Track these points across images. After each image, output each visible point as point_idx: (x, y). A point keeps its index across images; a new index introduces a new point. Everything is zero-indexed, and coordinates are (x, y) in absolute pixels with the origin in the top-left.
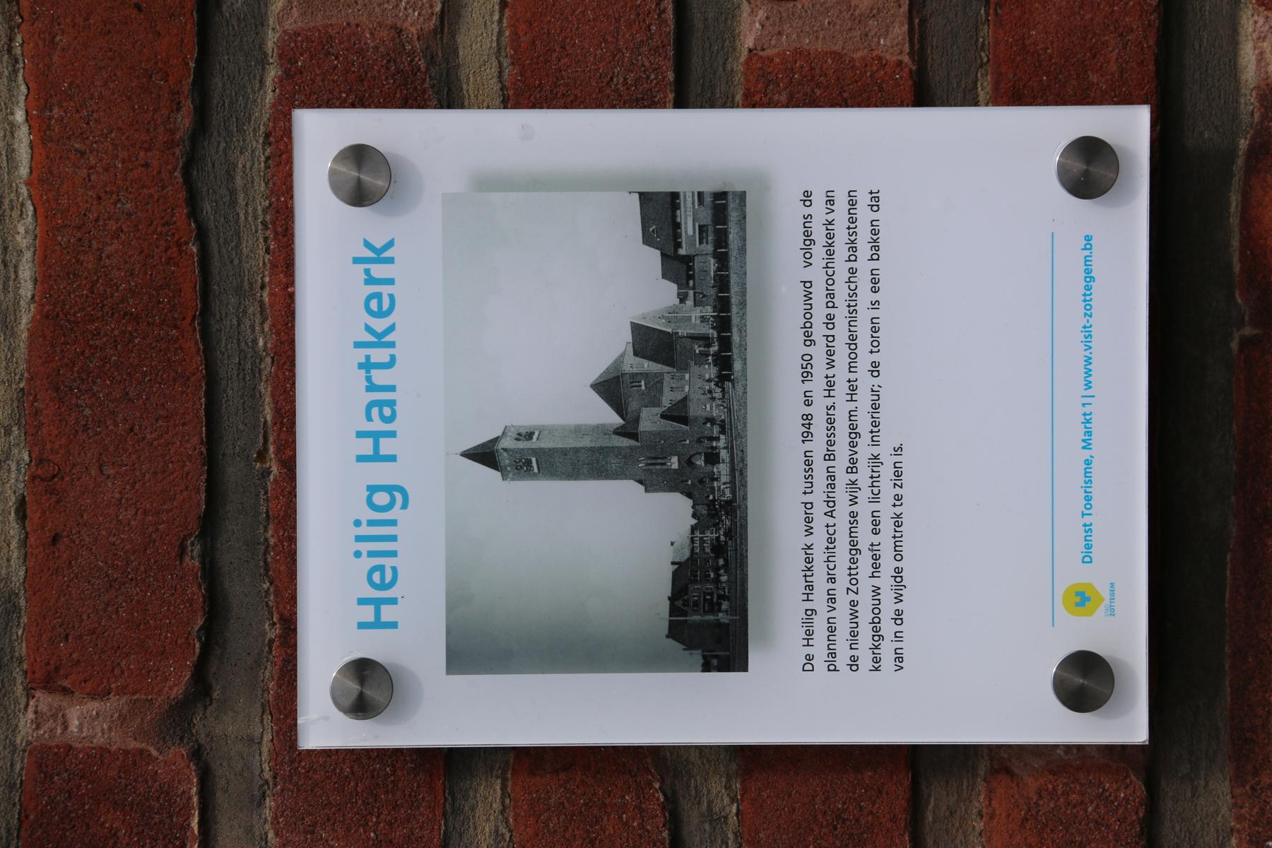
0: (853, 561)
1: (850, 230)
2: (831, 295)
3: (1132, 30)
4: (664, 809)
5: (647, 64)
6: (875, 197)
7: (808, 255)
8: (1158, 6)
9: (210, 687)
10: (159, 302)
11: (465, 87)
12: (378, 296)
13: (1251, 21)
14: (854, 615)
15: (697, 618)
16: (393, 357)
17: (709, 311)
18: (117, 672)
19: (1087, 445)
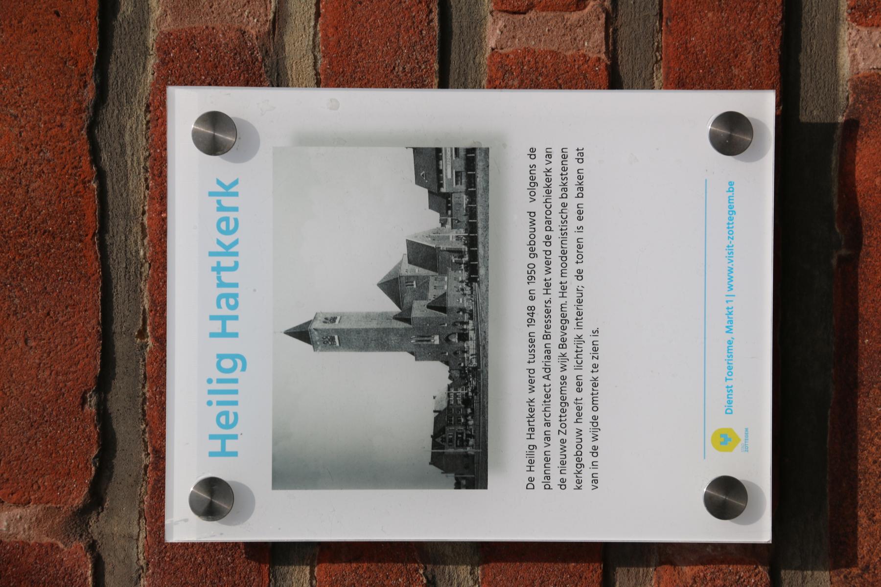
0: (563, 411)
1: (563, 176)
2: (549, 222)
3: (763, 38)
5: (419, 58)
6: (580, 153)
8: (781, 22)
10: (69, 223)
11: (289, 72)
12: (227, 219)
13: (847, 33)
14: (563, 449)
15: (451, 450)
16: (236, 263)
17: (462, 232)
19: (729, 330)
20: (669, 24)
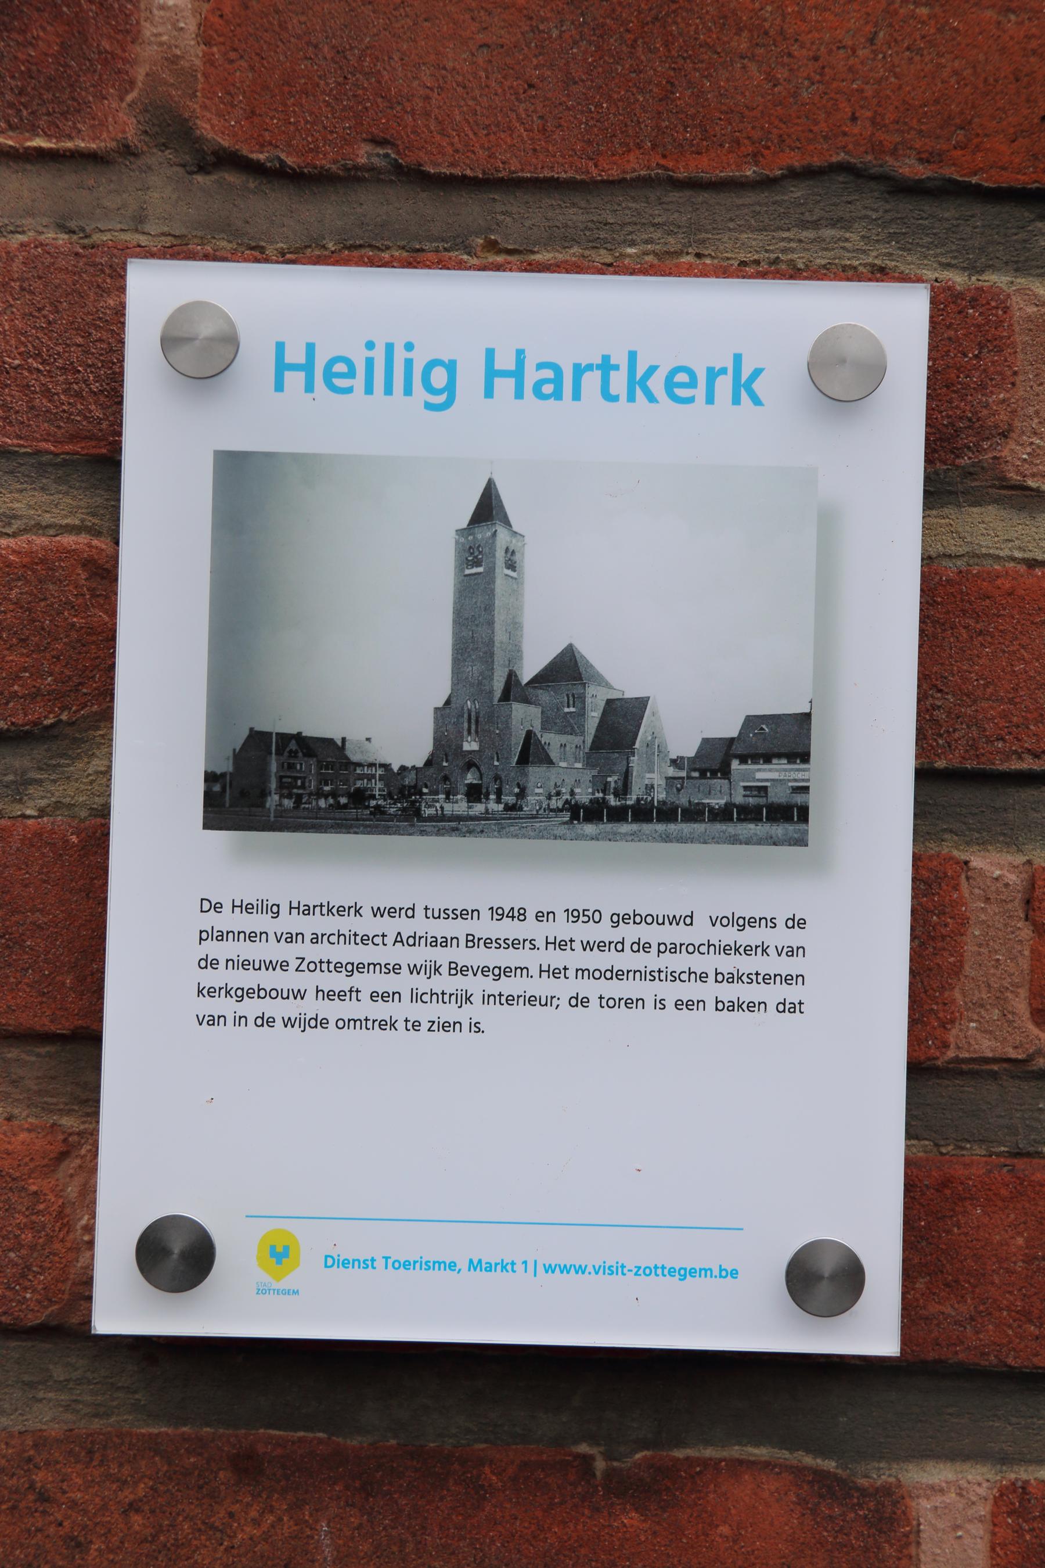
0: (338, 967)
1: (755, 975)
2: (674, 949)
3: (977, 1333)
4: (35, 724)
5: (956, 735)
6: (795, 1008)
7: (725, 921)
8: (1006, 1365)
9: (208, 173)
10: (686, 127)
11: (934, 512)
12: (693, 383)
13: (979, 1480)
14: (270, 966)
15: (274, 767)
16: (615, 399)
17: (660, 795)
18: (233, 55)
20: (1006, 1169)
